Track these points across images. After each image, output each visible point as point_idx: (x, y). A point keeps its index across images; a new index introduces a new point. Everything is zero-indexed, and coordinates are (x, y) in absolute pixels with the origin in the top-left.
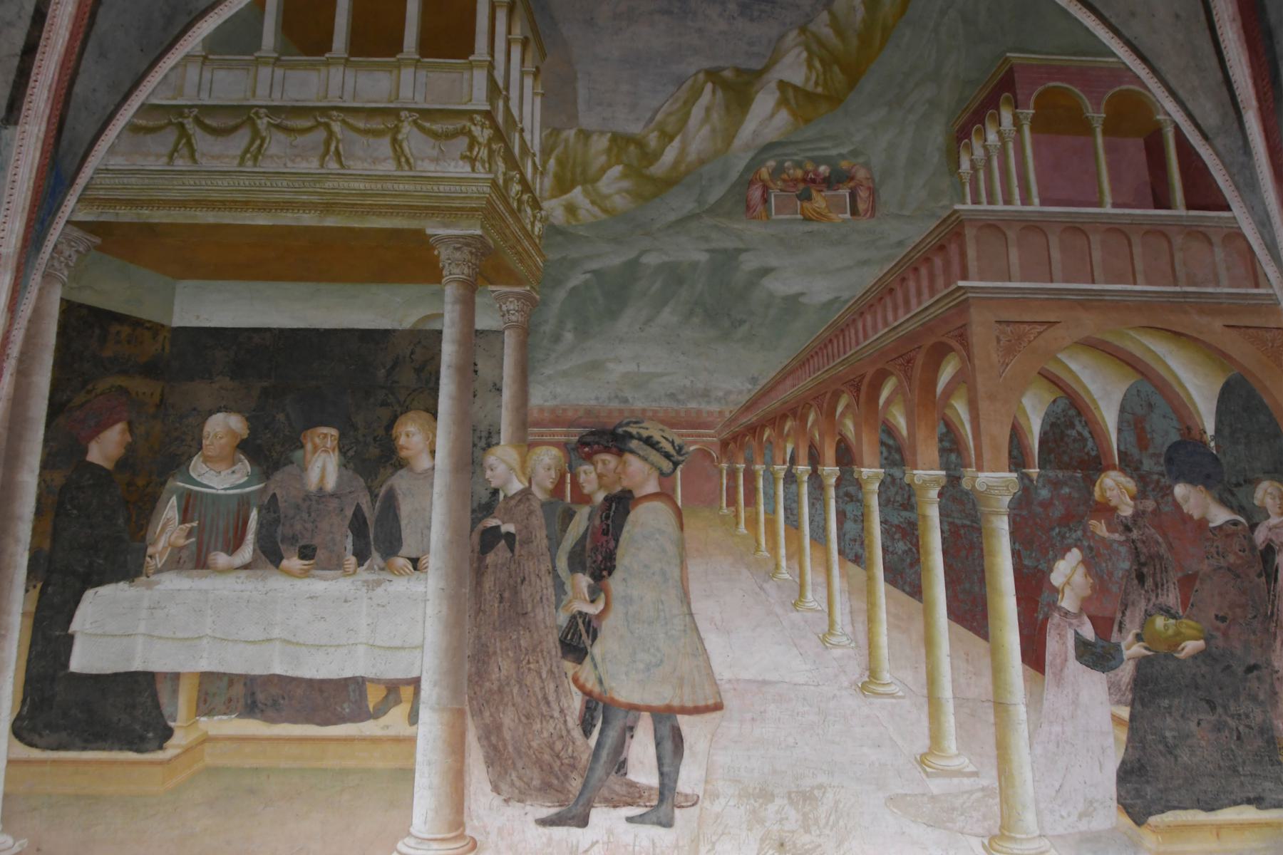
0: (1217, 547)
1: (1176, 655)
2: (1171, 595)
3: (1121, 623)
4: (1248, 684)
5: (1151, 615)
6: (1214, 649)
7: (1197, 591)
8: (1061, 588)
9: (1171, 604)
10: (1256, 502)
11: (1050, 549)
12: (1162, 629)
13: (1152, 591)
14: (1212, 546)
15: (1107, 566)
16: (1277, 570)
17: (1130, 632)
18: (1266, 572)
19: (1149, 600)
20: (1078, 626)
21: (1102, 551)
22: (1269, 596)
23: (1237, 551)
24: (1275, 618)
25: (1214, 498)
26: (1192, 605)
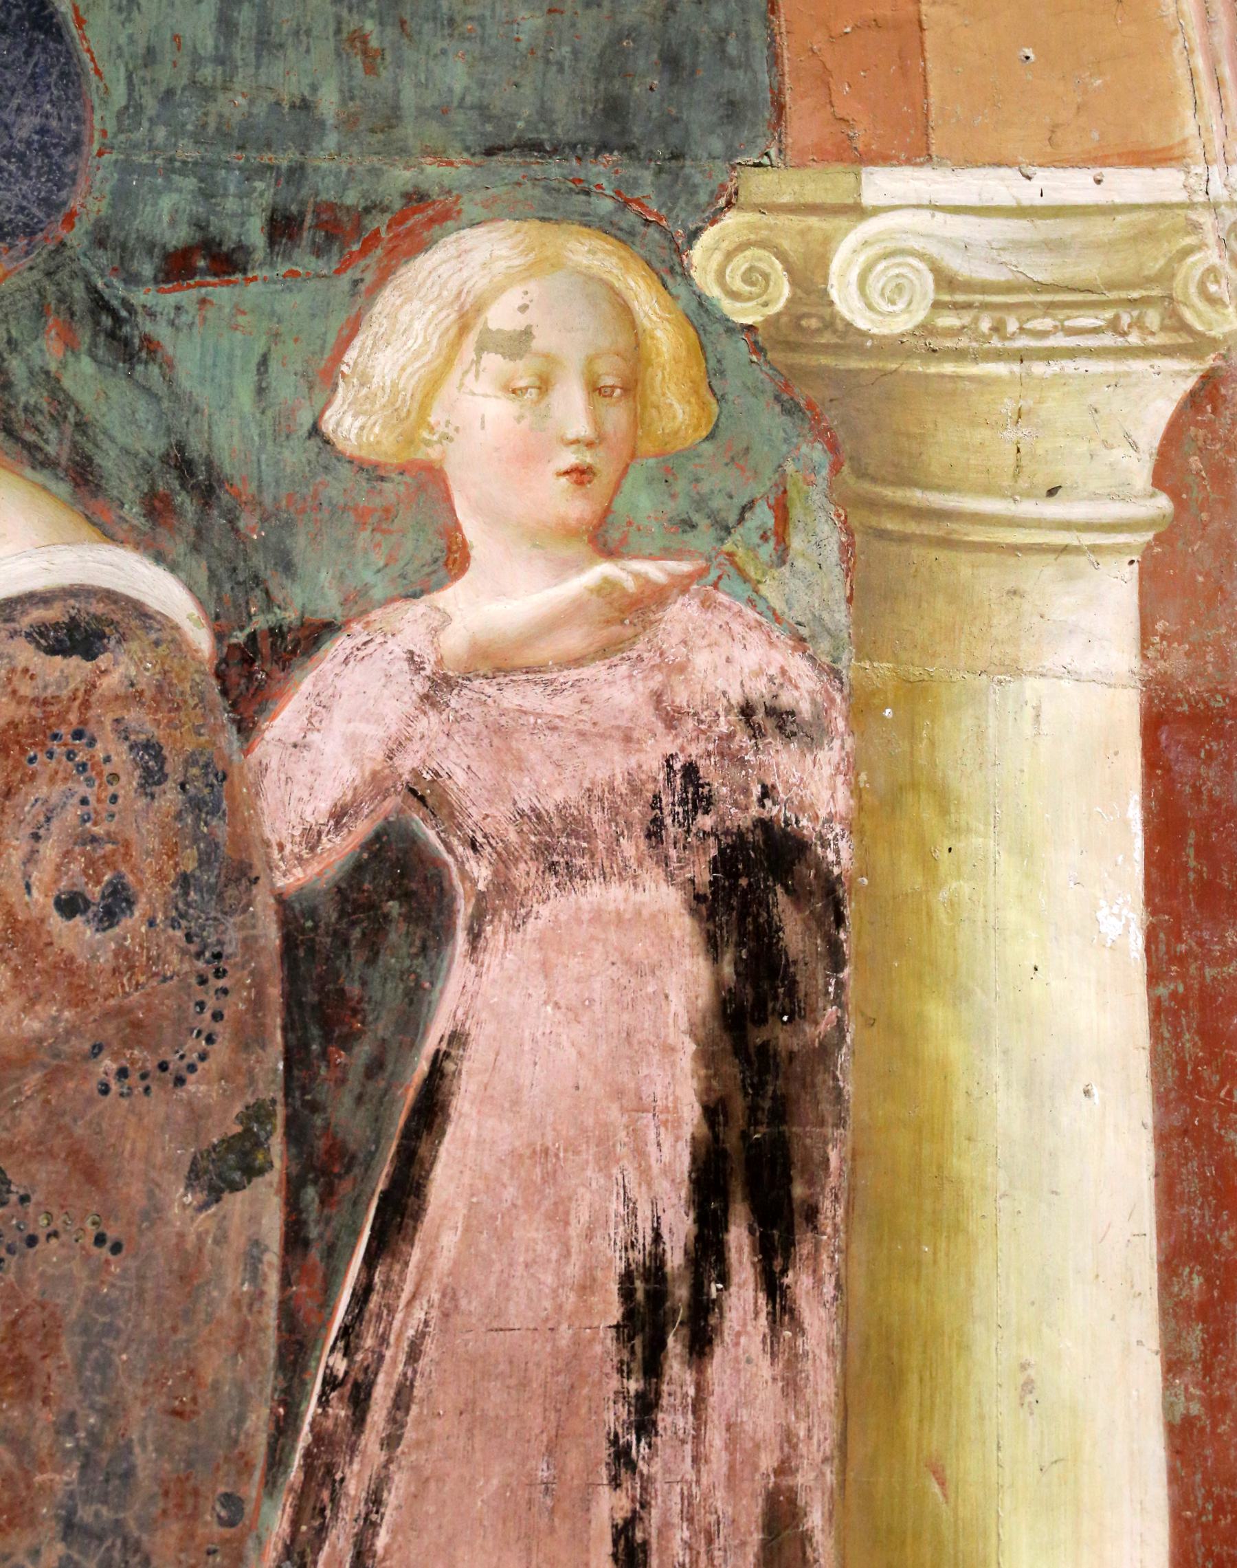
18: (296, 1133)
22: (290, 1401)
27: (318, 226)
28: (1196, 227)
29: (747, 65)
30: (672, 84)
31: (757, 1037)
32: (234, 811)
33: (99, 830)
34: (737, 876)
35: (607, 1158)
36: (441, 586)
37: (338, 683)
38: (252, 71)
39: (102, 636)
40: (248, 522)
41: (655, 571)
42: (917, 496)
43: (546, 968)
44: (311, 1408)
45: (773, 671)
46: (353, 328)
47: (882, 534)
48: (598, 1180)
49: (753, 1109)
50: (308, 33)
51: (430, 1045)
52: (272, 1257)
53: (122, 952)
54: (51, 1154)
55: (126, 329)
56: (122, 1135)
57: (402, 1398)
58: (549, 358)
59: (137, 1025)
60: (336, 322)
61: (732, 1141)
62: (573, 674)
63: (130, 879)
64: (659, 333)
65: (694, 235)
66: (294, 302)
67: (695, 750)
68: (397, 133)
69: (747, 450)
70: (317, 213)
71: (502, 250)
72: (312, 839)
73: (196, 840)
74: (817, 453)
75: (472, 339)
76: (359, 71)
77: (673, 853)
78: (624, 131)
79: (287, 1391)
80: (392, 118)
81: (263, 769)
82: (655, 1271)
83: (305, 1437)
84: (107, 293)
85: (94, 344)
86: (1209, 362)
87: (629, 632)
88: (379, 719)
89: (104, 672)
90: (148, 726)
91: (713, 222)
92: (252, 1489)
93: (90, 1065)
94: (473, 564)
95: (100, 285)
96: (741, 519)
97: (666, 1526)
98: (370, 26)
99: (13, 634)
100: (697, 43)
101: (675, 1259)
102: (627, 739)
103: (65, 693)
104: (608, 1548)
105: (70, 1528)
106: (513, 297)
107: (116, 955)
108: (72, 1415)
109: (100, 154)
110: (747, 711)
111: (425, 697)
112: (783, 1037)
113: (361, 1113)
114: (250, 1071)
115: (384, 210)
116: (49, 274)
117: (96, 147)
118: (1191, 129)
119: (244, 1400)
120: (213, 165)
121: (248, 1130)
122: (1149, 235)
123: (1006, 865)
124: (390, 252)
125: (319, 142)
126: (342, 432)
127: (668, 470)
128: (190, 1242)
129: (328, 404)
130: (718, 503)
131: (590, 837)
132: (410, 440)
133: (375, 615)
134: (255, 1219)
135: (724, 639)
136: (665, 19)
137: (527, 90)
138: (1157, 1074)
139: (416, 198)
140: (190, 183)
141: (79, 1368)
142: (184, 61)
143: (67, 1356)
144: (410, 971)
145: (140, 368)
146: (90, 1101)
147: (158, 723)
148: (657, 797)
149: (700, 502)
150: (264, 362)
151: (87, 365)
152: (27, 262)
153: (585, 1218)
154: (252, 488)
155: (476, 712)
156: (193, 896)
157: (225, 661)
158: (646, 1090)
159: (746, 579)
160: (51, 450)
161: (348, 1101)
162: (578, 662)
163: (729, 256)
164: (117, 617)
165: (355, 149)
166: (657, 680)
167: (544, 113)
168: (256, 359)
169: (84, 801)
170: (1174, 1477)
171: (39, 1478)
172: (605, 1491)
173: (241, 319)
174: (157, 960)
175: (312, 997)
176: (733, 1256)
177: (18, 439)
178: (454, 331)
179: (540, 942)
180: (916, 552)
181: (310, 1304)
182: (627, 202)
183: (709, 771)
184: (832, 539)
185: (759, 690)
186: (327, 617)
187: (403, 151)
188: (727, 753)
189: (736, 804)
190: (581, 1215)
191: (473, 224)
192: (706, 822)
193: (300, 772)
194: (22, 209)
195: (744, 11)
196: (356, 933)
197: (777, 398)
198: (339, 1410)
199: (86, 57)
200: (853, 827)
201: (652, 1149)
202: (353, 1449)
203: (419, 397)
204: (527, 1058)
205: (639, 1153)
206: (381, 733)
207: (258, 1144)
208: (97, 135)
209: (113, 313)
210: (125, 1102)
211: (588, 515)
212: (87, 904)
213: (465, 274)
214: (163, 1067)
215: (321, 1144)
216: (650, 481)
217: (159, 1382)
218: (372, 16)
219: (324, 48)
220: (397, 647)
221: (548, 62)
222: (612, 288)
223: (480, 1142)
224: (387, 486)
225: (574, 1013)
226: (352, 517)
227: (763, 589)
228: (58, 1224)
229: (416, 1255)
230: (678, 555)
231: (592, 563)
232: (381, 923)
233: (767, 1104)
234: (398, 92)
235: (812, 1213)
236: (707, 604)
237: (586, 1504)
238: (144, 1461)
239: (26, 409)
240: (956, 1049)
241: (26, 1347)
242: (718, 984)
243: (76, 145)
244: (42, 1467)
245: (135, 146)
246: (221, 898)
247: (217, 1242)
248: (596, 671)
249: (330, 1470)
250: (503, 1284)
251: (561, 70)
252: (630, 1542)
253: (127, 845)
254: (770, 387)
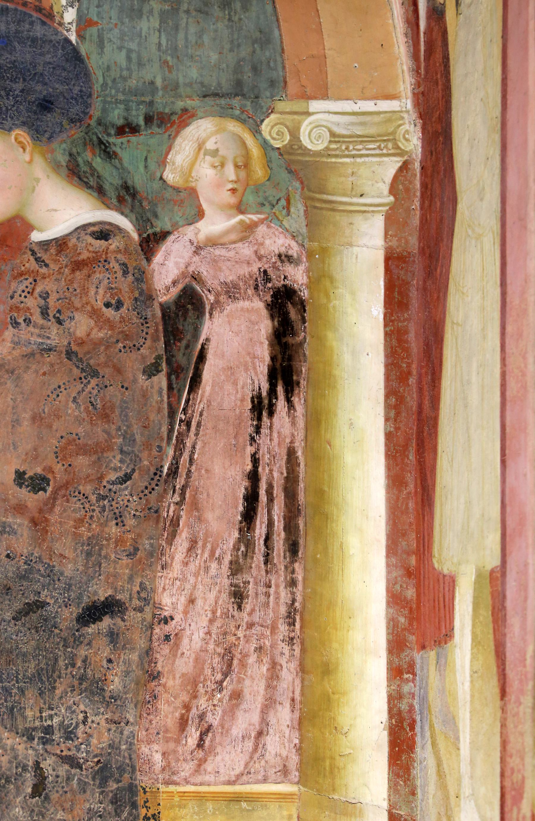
0: (45, 296)
4: (82, 652)
10: (170, 176)
14: (31, 293)
16: (202, 357)
18: (169, 362)
23: (100, 304)
24: (180, 482)
25: (56, 167)
27: (158, 119)
28: (403, 118)
29: (276, 69)
30: (255, 75)
31: (284, 340)
32: (147, 281)
33: (113, 286)
34: (278, 299)
35: (246, 370)
36: (197, 222)
37: (172, 248)
38: (137, 72)
39: (109, 235)
40: (145, 203)
41: (255, 218)
42: (325, 197)
43: (229, 323)
44: (177, 427)
45: (286, 245)
46: (170, 149)
47: (315, 207)
48: (244, 375)
49: (283, 358)
50: (152, 61)
51: (201, 341)
52: (165, 392)
53: (121, 317)
54: (108, 366)
55: (108, 149)
56: (126, 362)
57: (199, 425)
58: (224, 157)
59: (127, 335)
60: (165, 147)
61: (278, 366)
62: (234, 246)
63: (122, 298)
64: (253, 150)
65: (262, 121)
66: (153, 141)
67: (266, 266)
68: (178, 91)
69: (278, 184)
70: (158, 115)
71: (209, 126)
72: (168, 289)
73: (138, 289)
74: (297, 185)
75: (202, 152)
76: (167, 73)
77: (261, 293)
78: (242, 90)
79: (171, 423)
80: (176, 87)
81: (154, 271)
82: (259, 396)
83: (176, 433)
84: (102, 139)
85: (100, 154)
86: (406, 158)
87: (248, 234)
88: (183, 257)
89: (111, 244)
90: (123, 259)
91: (268, 117)
92: (164, 444)
93: (116, 345)
94: (205, 216)
95: (100, 136)
96: (277, 203)
97: (263, 455)
98: (169, 58)
99: (86, 234)
100: (261, 62)
101: (264, 394)
102: (248, 263)
103: (101, 250)
104: (250, 459)
105: (122, 452)
106: (213, 140)
107: (120, 318)
108: (120, 427)
109: (97, 98)
110: (280, 256)
111: (195, 252)
112: (290, 340)
113: (185, 358)
114: (156, 347)
115: (176, 114)
116: (86, 133)
117: (96, 96)
118: (402, 88)
119: (161, 424)
120: (129, 101)
121: (157, 361)
122: (389, 120)
123: (348, 297)
124: (179, 126)
125: (157, 94)
126: (169, 179)
127: (257, 189)
128: (145, 388)
129: (164, 171)
130: (271, 199)
131: (240, 289)
132: (187, 181)
133: (180, 229)
134: (160, 382)
135: (273, 236)
136: (252, 55)
137: (214, 78)
138: (385, 350)
139: (185, 110)
140: (122, 106)
141: (120, 415)
142: (118, 69)
143: (117, 413)
144: (195, 323)
145: (113, 160)
146: (117, 354)
147: (126, 258)
148: (257, 279)
149: (266, 198)
150: (146, 159)
151: (99, 160)
152: (80, 130)
153: (241, 384)
154: (145, 194)
155: (208, 256)
156: (138, 303)
157: (142, 242)
158: (256, 353)
159: (279, 220)
160: (91, 183)
161: (181, 355)
162: (234, 242)
163: (272, 127)
164: (113, 230)
165: (167, 96)
166: (256, 247)
167: (219, 84)
168: (144, 158)
169: (109, 278)
170: (386, 445)
171: (113, 440)
172: (249, 447)
173: (139, 146)
174: (131, 319)
175: (170, 329)
176: (279, 393)
177: (83, 181)
178: (197, 149)
179: (228, 316)
180: (324, 212)
181: (175, 403)
182: (243, 111)
183: (270, 272)
184: (302, 209)
185: (283, 250)
186: (167, 230)
187: (181, 96)
188: (275, 267)
189: (277, 281)
190: (241, 383)
191: (201, 118)
192: (270, 285)
193: (163, 272)
194: (77, 114)
195: (275, 53)
196: (181, 313)
197: (286, 169)
198: (184, 427)
199: (91, 69)
200: (308, 287)
201: (258, 367)
202: (188, 436)
203: (189, 168)
204: (226, 345)
205: (255, 368)
206: (184, 261)
207: (159, 365)
208: (96, 93)
209: (104, 144)
210: (126, 354)
211: (236, 202)
212: (112, 305)
213: (200, 133)
214: (134, 346)
215: (175, 365)
216: (252, 192)
217: (140, 420)
218: (169, 55)
219: (156, 65)
220: (186, 238)
221: (219, 69)
222: (240, 137)
223: (214, 365)
224: (181, 194)
225: (237, 334)
226: (172, 203)
227: (284, 223)
228: (112, 383)
229: (200, 392)
230: (261, 213)
231: (237, 215)
232: (186, 311)
233: (287, 357)
234: (178, 78)
235: (298, 383)
236: (269, 227)
237: (244, 449)
238: (138, 437)
239: (84, 172)
240: (334, 344)
241: (107, 411)
242: (274, 327)
243: (90, 96)
244: (114, 438)
245: (107, 95)
246: (145, 304)
247: (151, 388)
248: (240, 245)
249: (182, 441)
250: (222, 399)
251: (223, 71)
252: (255, 458)
253: (120, 290)
254: (284, 166)
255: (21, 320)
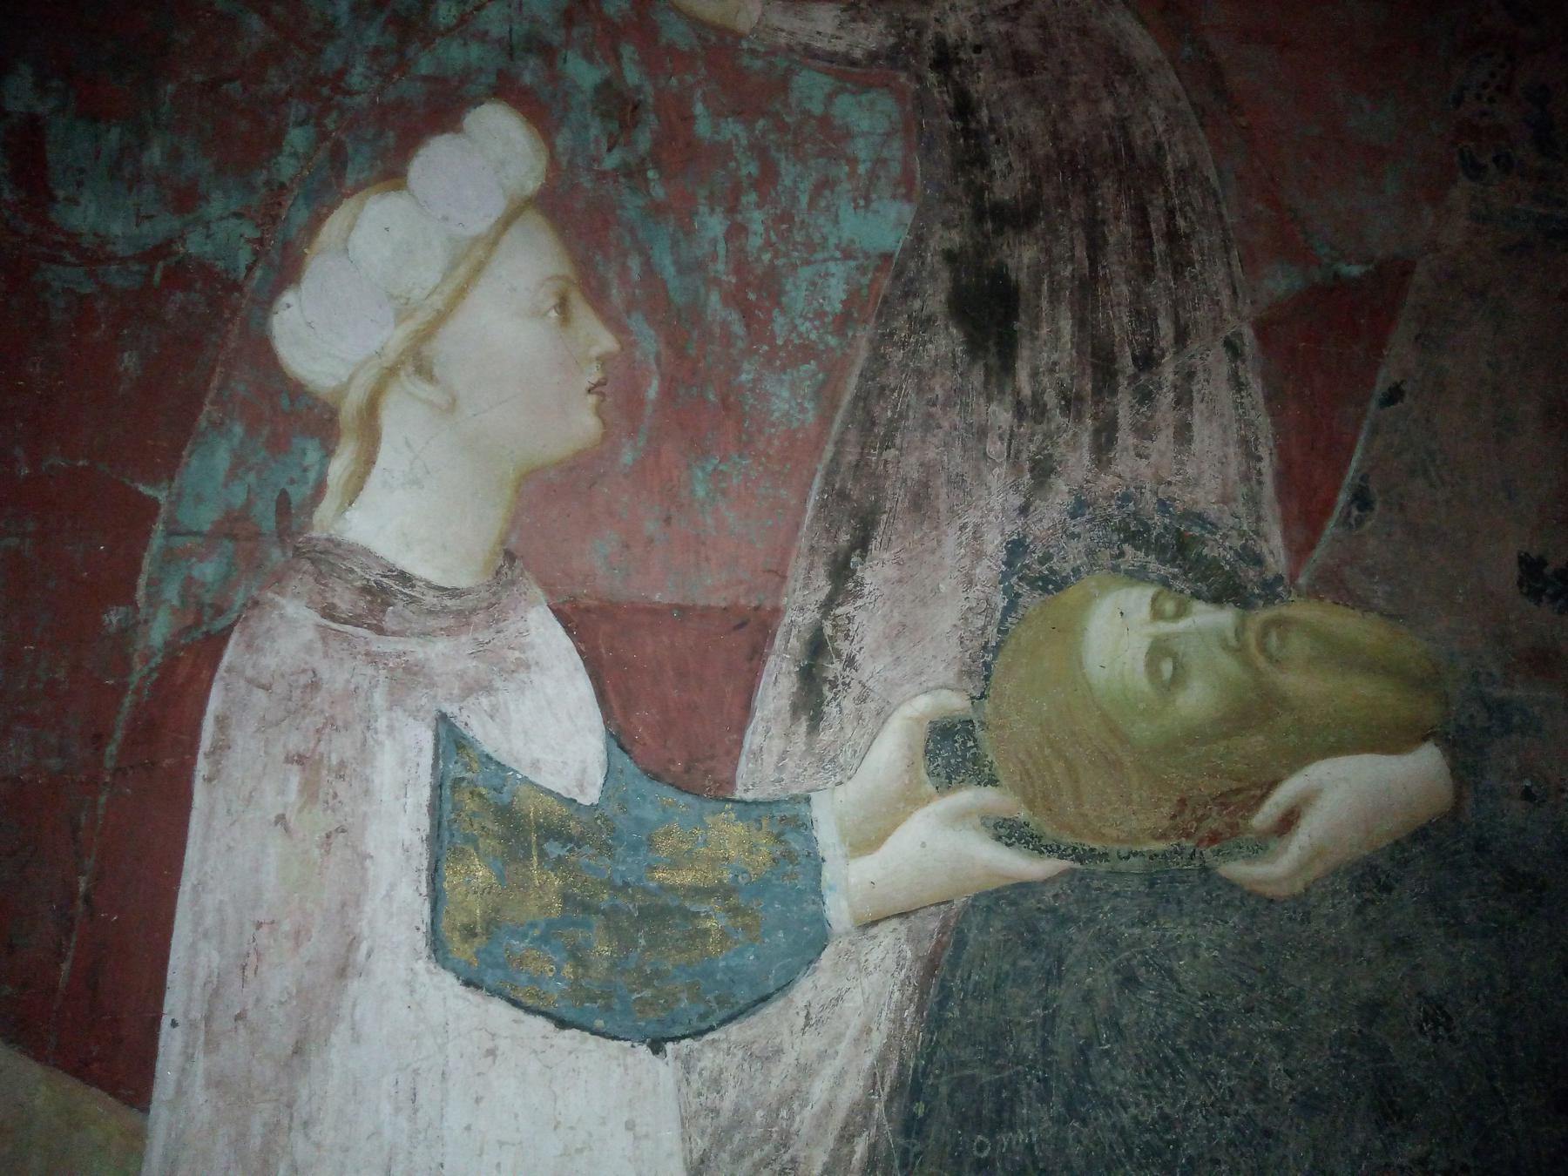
1: (1237, 870)
2: (1205, 435)
3: (817, 647)
5: (1051, 583)
6: (1516, 810)
7: (1394, 395)
8: (350, 408)
9: (1205, 498)
11: (297, 109)
12: (1141, 682)
13: (1071, 403)
15: (737, 231)
17: (882, 716)
19: (1043, 471)
20: (474, 688)
21: (703, 128)
26: (1362, 499)
255: (1486, 159)
